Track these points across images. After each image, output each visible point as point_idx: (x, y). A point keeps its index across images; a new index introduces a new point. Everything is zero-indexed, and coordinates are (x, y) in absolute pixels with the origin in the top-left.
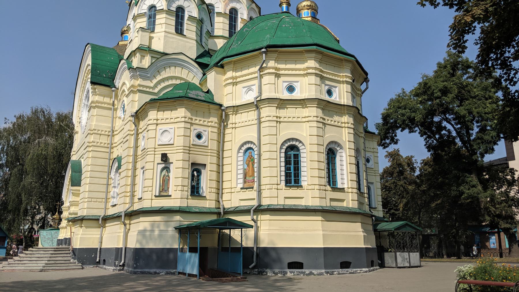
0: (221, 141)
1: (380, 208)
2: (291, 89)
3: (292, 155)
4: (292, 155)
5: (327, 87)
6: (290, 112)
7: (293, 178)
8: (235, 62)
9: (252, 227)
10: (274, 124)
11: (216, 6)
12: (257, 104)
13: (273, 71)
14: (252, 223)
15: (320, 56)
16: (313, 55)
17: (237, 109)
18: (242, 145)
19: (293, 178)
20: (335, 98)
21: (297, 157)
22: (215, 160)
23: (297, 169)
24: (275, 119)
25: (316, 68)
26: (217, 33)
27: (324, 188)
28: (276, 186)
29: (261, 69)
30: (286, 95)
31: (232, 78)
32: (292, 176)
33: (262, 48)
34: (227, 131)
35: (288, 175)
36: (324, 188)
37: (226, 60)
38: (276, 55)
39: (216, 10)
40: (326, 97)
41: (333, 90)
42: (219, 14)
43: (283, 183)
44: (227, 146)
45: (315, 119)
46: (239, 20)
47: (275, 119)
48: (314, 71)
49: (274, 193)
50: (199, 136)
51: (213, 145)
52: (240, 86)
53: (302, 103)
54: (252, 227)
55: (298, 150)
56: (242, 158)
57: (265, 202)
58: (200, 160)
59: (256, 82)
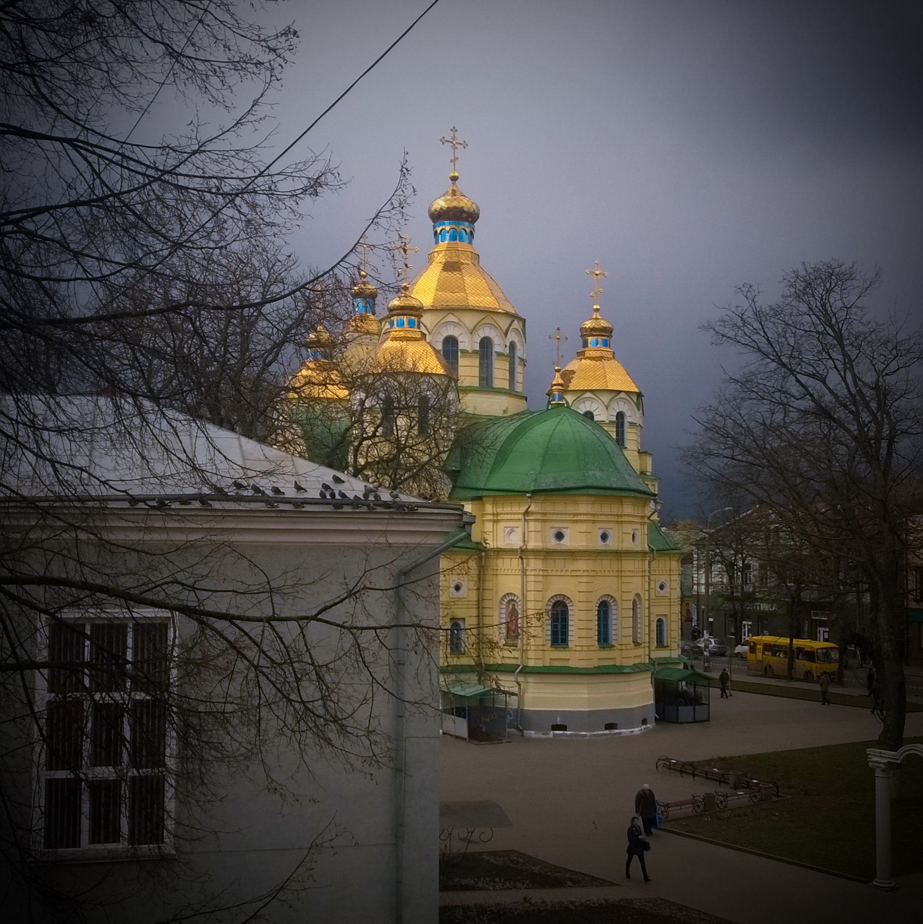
0: (480, 589)
1: (674, 646)
2: (560, 536)
3: (559, 613)
4: (559, 613)
5: (600, 532)
6: (559, 564)
7: (560, 637)
8: (494, 496)
9: (516, 695)
10: (540, 579)
11: (460, 339)
12: (523, 553)
13: (539, 517)
14: (515, 690)
15: (593, 499)
16: (585, 498)
17: (499, 552)
18: (504, 596)
19: (560, 637)
20: (612, 544)
21: (565, 613)
22: (474, 612)
23: (565, 627)
24: (541, 573)
25: (587, 514)
26: (464, 382)
27: (591, 648)
28: (541, 648)
29: (526, 513)
30: (553, 544)
31: (493, 514)
32: (560, 637)
33: (527, 492)
34: (488, 578)
35: (554, 634)
36: (591, 648)
37: (485, 493)
38: (543, 498)
39: (461, 346)
40: (599, 545)
41: (610, 532)
42: (464, 352)
43: (549, 643)
44: (488, 595)
45: (586, 574)
46: (494, 355)
47: (541, 573)
48: (585, 518)
49: (540, 654)
50: (458, 588)
51: (473, 596)
52: (501, 525)
53: (572, 554)
54: (516, 695)
55: (565, 605)
56: (504, 611)
57: (531, 663)
58: (460, 613)
59: (520, 524)
